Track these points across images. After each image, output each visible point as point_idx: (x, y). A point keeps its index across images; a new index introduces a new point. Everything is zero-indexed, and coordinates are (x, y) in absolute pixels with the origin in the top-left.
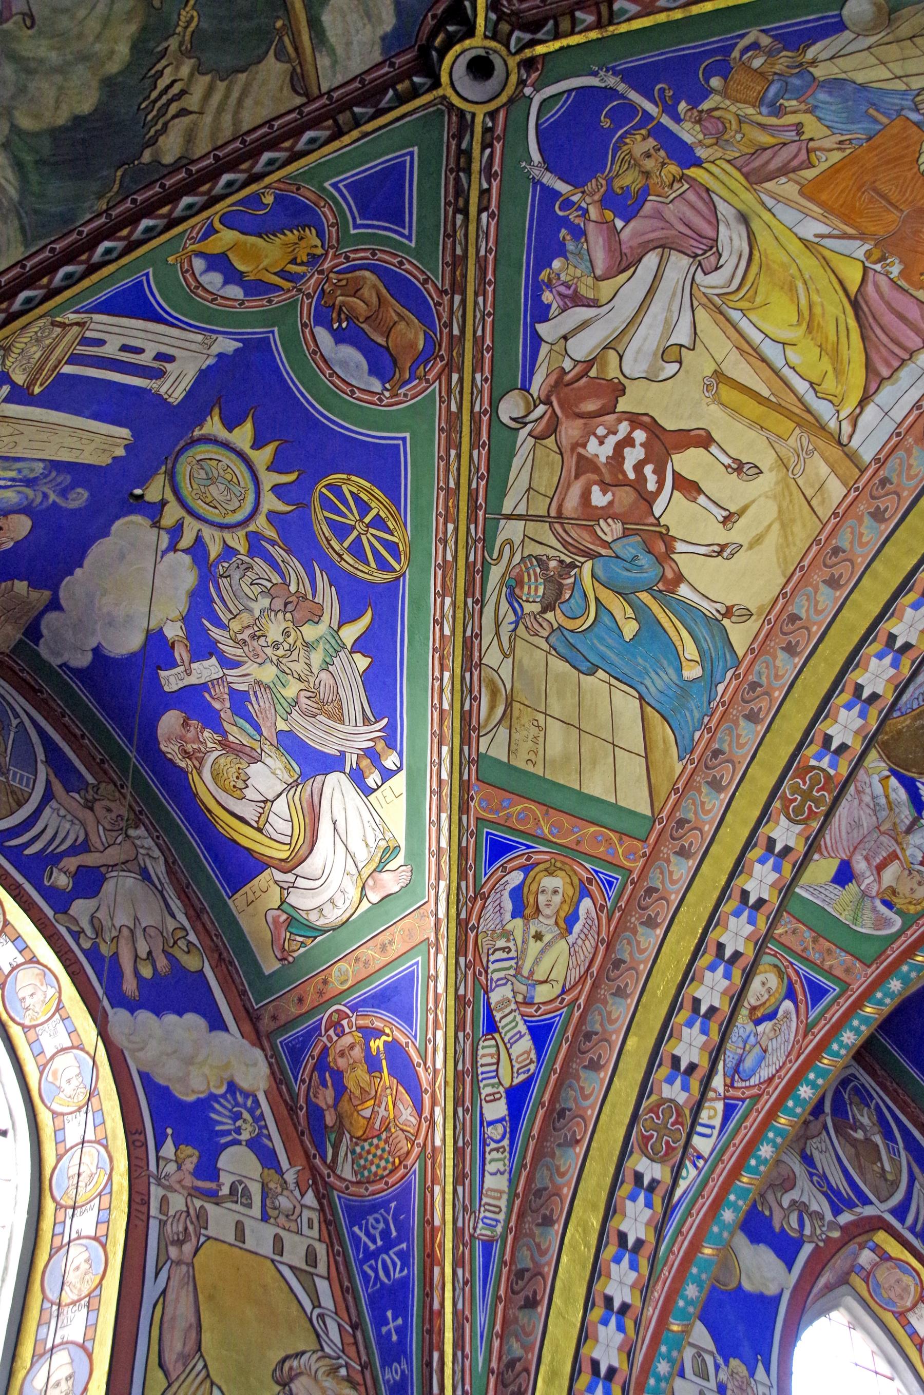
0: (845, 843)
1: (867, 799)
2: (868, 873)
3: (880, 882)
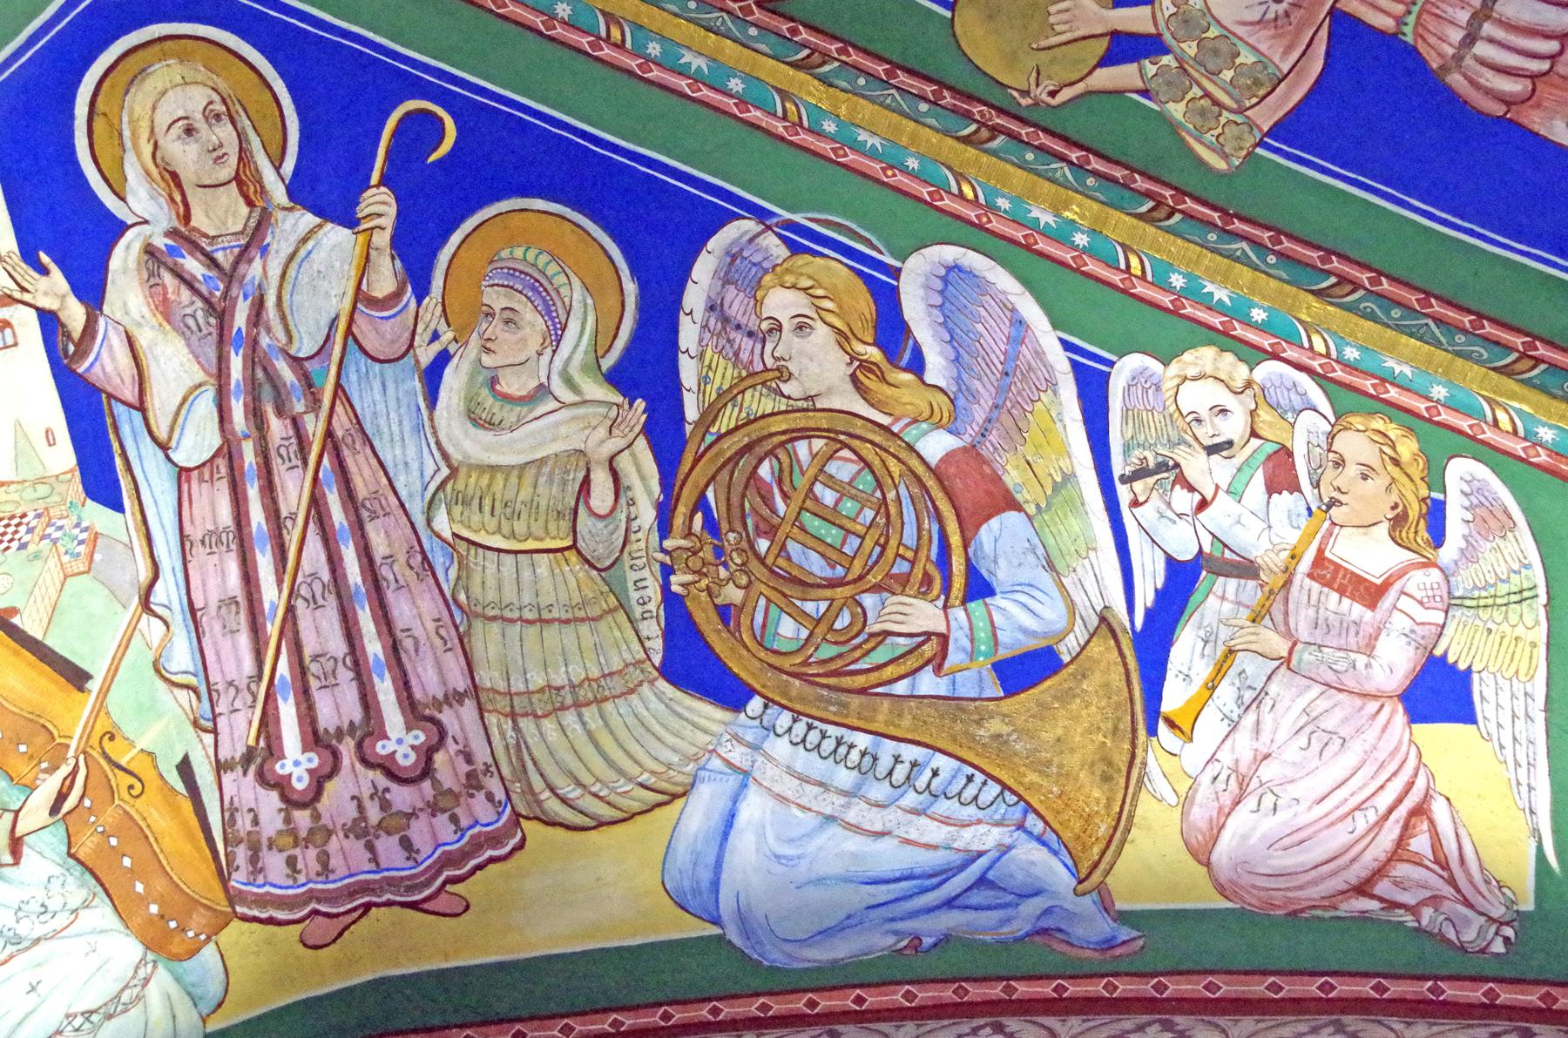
0: (1371, 735)
1: (1244, 745)
2: (1399, 622)
3: (1401, 574)
